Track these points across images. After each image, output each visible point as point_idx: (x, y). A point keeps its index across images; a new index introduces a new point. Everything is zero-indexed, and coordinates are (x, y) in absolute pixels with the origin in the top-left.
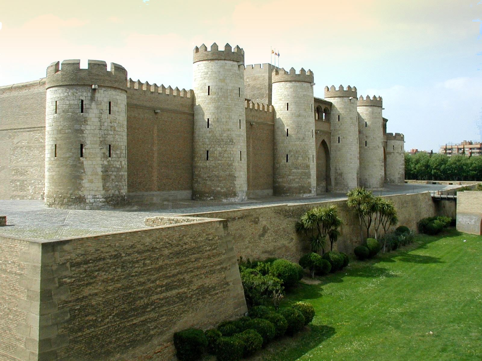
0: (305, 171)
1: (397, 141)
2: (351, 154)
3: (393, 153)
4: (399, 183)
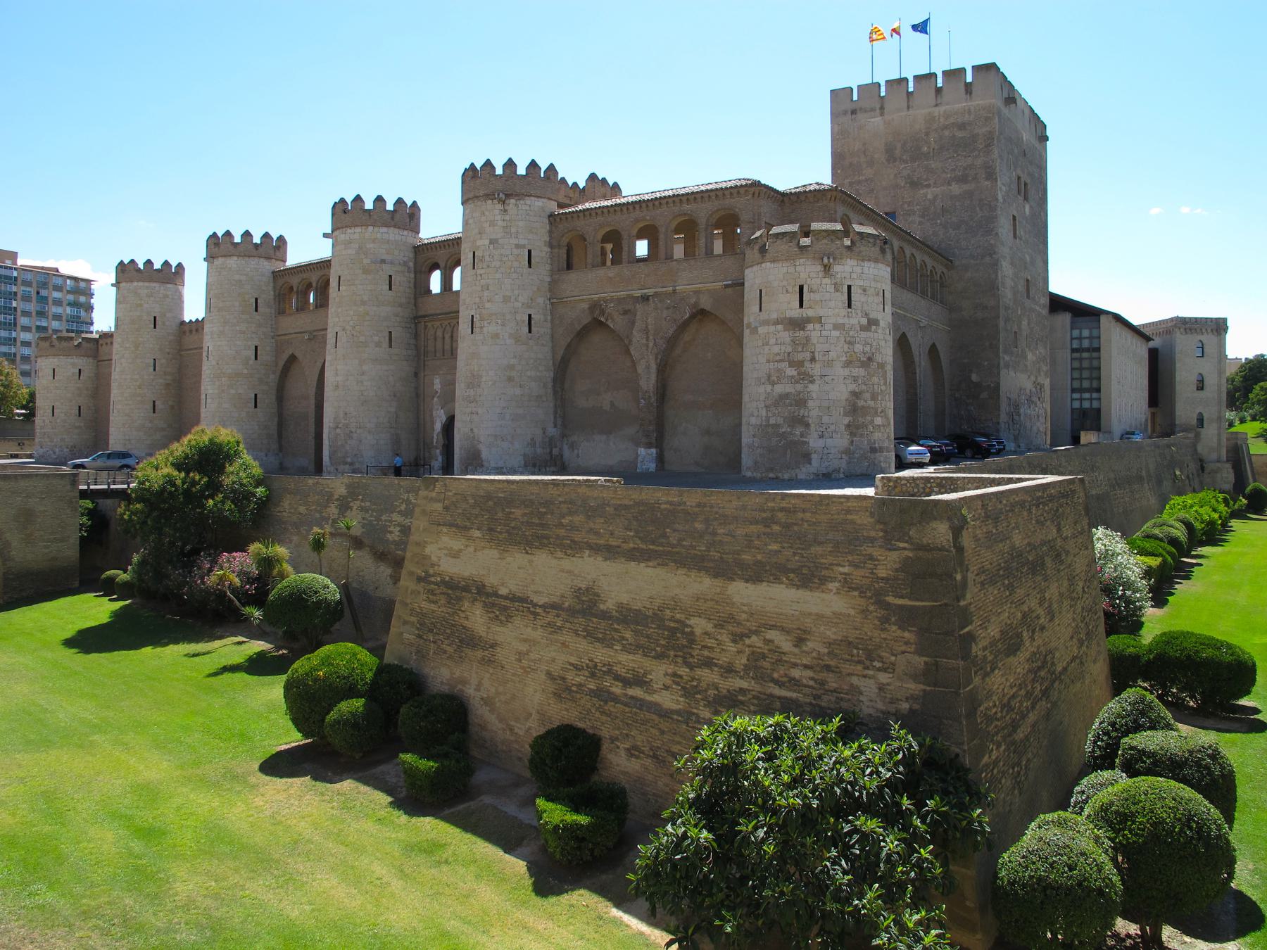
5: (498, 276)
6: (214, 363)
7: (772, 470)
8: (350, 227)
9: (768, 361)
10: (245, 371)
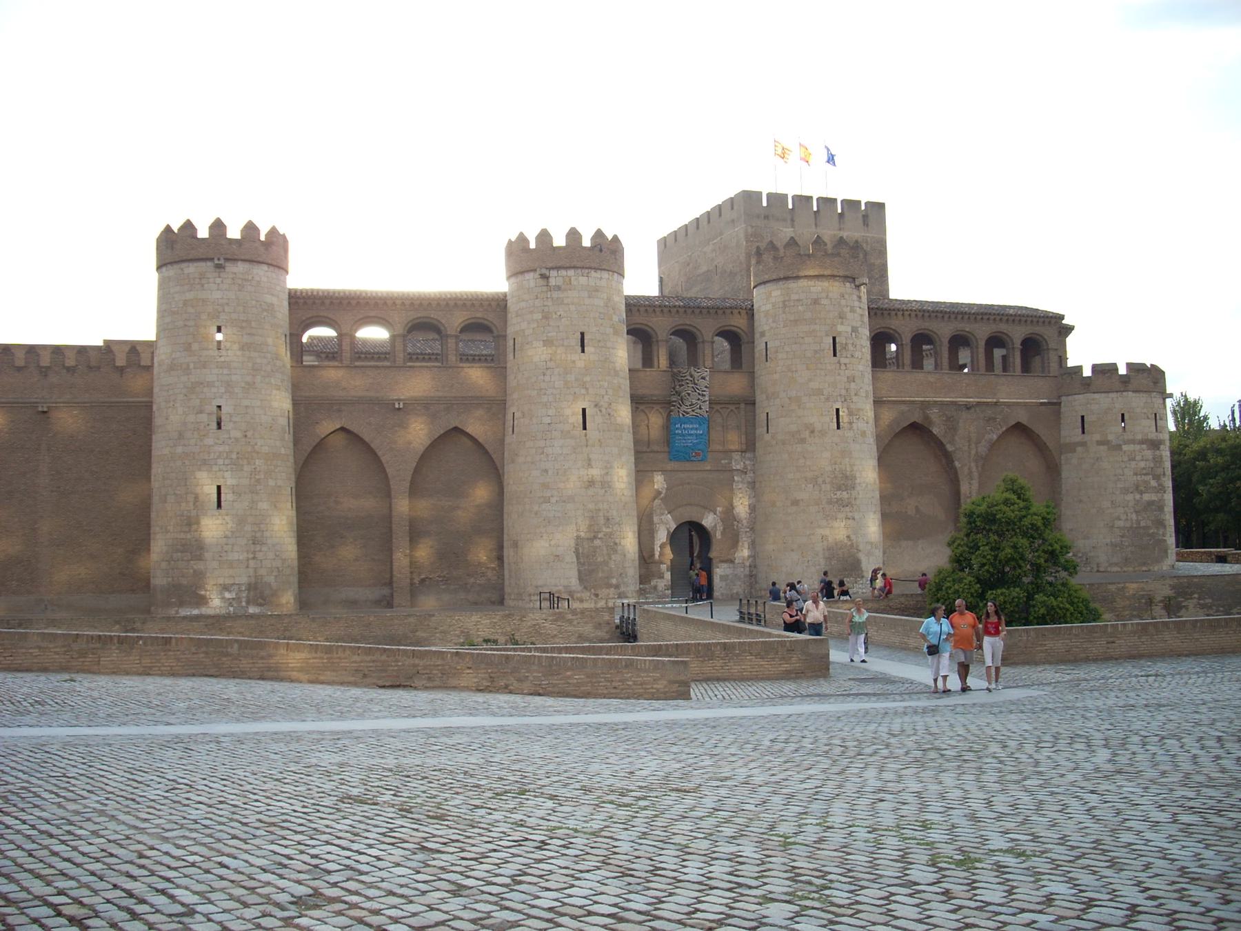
0: (182, 536)
1: (1096, 396)
2: (546, 471)
3: (1084, 444)
4: (1111, 565)
5: (861, 368)
6: (239, 434)
7: (1144, 564)
8: (596, 269)
9: (1136, 474)
10: (283, 451)
